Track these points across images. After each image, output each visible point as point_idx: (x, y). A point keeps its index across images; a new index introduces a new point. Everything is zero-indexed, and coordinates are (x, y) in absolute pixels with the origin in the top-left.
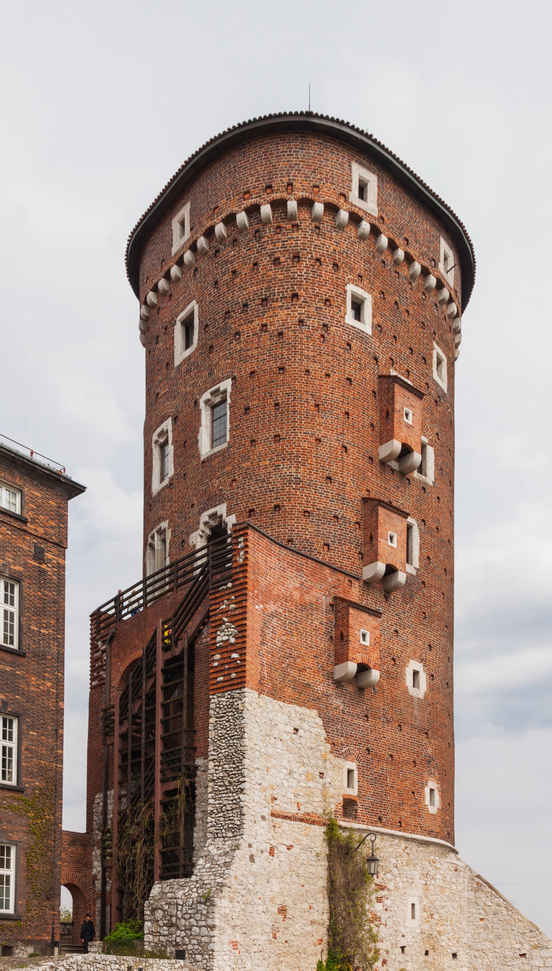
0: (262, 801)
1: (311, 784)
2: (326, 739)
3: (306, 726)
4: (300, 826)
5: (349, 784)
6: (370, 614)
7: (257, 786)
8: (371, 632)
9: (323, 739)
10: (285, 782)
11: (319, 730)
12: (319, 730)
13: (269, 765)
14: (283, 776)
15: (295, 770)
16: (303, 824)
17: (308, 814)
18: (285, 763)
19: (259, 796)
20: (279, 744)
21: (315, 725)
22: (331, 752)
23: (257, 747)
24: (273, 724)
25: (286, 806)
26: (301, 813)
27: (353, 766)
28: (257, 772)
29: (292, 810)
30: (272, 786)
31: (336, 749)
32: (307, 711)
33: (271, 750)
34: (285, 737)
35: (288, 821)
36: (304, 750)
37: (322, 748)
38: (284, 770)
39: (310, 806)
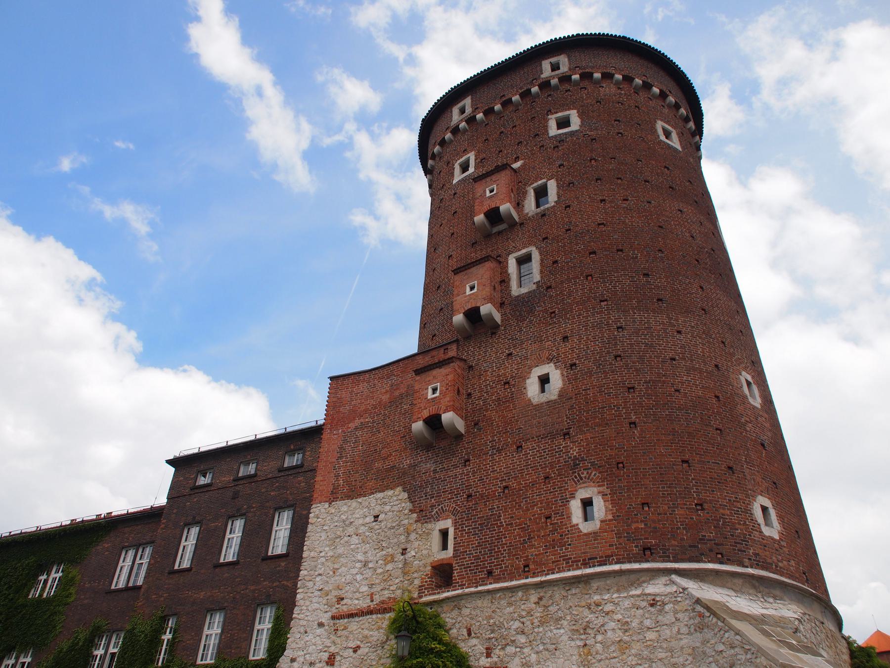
0: (322, 607)
1: (389, 567)
2: (410, 511)
3: (388, 508)
4: (370, 620)
5: (445, 547)
6: (440, 367)
7: (319, 593)
8: (441, 383)
9: (406, 511)
10: (359, 577)
11: (403, 505)
12: (403, 505)
13: (336, 566)
14: (354, 571)
15: (371, 558)
16: (374, 616)
17: (383, 602)
18: (360, 557)
19: (319, 603)
20: (355, 540)
21: (397, 502)
22: (416, 521)
23: (322, 554)
24: (347, 523)
25: (357, 602)
26: (372, 605)
27: (447, 524)
28: (318, 579)
29: (364, 603)
30: (338, 587)
31: (424, 515)
32: (390, 493)
33: (340, 550)
34: (362, 529)
35: (357, 619)
36: (383, 534)
37: (406, 522)
38: (358, 565)
39: (386, 592)
